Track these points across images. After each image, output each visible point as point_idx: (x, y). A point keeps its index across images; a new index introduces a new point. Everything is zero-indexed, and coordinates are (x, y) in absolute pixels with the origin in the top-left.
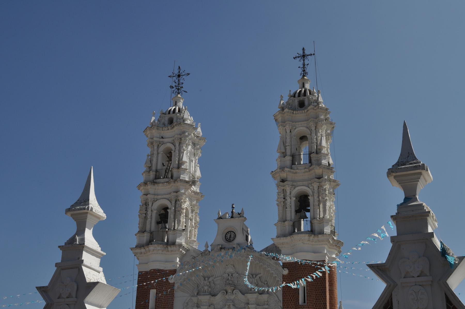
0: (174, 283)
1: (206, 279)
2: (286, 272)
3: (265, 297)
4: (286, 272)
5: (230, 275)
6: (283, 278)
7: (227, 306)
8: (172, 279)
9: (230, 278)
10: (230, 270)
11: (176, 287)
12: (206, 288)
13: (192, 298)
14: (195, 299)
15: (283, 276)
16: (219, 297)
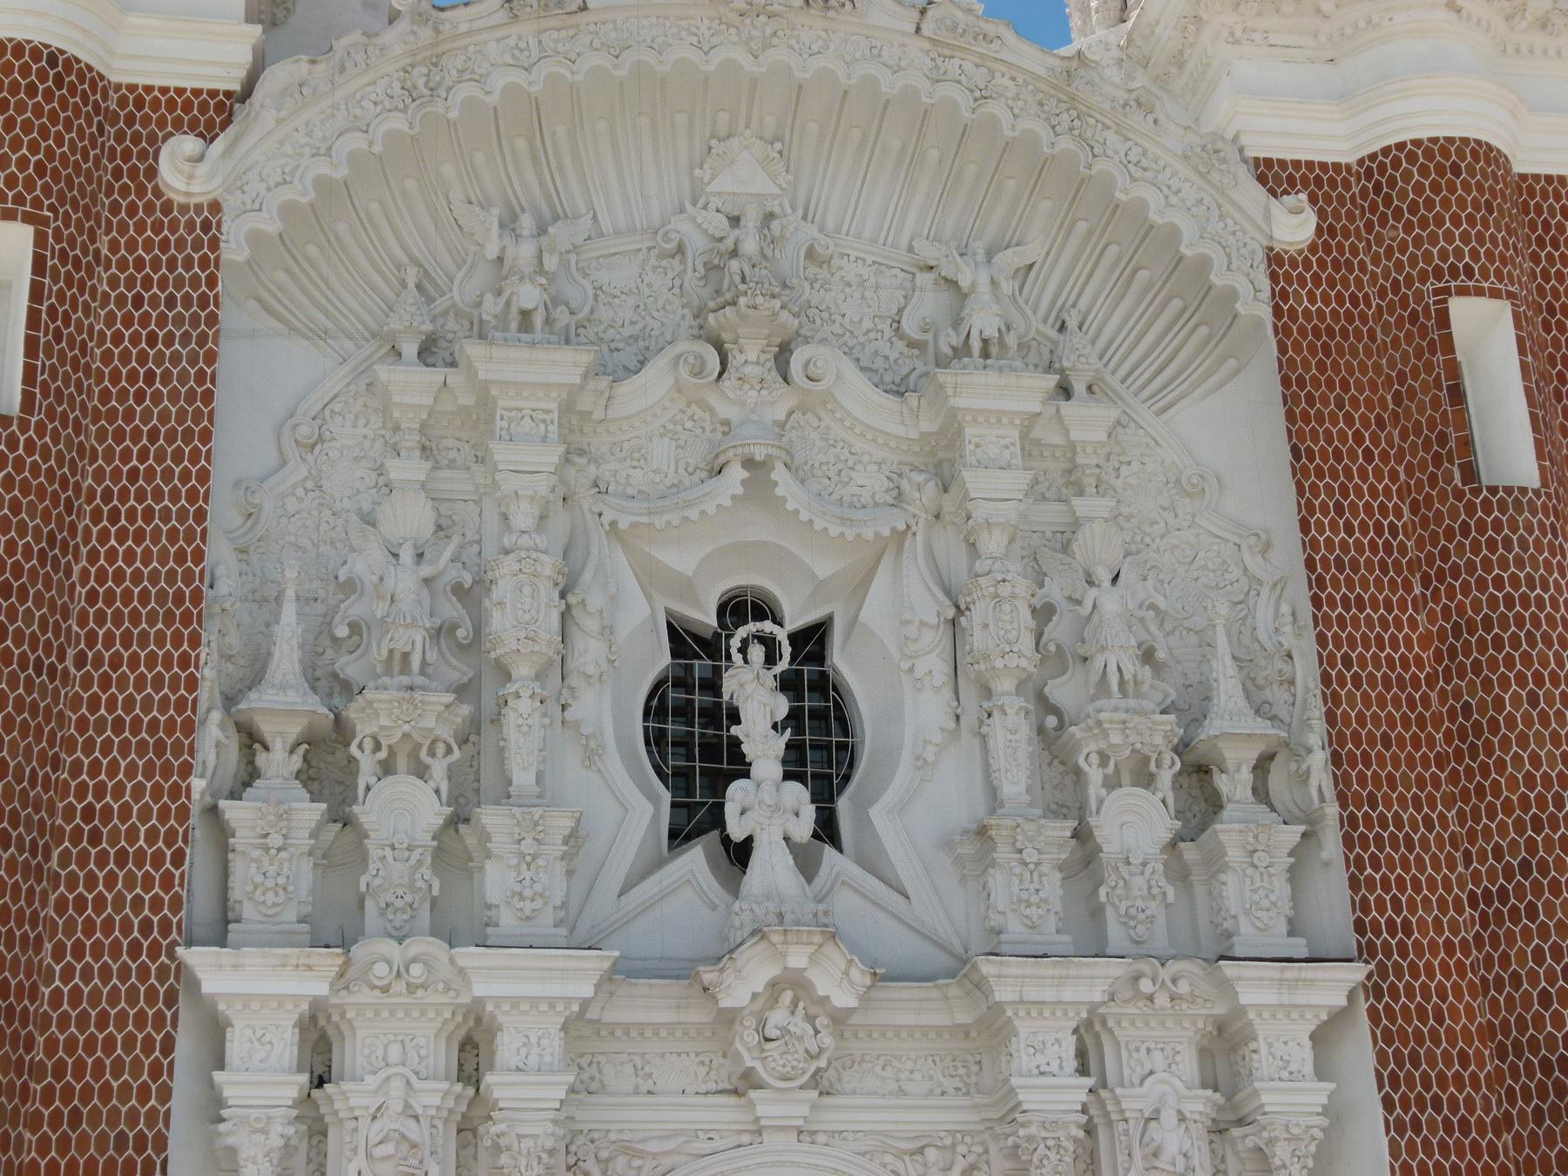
0: (215, 207)
1: (527, 223)
2: (1295, 226)
3: (1087, 421)
4: (1295, 226)
5: (751, 221)
6: (1274, 277)
7: (736, 473)
8: (184, 170)
9: (750, 246)
10: (745, 177)
11: (234, 250)
12: (529, 295)
13: (386, 373)
14: (412, 385)
15: (1274, 259)
16: (652, 387)
